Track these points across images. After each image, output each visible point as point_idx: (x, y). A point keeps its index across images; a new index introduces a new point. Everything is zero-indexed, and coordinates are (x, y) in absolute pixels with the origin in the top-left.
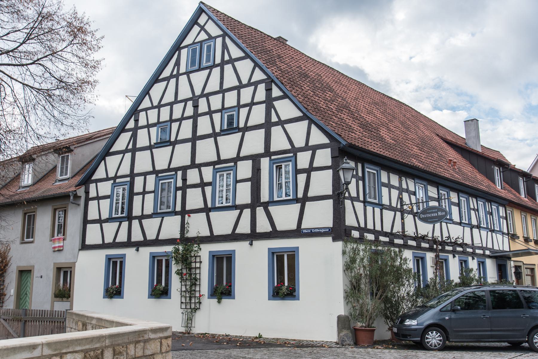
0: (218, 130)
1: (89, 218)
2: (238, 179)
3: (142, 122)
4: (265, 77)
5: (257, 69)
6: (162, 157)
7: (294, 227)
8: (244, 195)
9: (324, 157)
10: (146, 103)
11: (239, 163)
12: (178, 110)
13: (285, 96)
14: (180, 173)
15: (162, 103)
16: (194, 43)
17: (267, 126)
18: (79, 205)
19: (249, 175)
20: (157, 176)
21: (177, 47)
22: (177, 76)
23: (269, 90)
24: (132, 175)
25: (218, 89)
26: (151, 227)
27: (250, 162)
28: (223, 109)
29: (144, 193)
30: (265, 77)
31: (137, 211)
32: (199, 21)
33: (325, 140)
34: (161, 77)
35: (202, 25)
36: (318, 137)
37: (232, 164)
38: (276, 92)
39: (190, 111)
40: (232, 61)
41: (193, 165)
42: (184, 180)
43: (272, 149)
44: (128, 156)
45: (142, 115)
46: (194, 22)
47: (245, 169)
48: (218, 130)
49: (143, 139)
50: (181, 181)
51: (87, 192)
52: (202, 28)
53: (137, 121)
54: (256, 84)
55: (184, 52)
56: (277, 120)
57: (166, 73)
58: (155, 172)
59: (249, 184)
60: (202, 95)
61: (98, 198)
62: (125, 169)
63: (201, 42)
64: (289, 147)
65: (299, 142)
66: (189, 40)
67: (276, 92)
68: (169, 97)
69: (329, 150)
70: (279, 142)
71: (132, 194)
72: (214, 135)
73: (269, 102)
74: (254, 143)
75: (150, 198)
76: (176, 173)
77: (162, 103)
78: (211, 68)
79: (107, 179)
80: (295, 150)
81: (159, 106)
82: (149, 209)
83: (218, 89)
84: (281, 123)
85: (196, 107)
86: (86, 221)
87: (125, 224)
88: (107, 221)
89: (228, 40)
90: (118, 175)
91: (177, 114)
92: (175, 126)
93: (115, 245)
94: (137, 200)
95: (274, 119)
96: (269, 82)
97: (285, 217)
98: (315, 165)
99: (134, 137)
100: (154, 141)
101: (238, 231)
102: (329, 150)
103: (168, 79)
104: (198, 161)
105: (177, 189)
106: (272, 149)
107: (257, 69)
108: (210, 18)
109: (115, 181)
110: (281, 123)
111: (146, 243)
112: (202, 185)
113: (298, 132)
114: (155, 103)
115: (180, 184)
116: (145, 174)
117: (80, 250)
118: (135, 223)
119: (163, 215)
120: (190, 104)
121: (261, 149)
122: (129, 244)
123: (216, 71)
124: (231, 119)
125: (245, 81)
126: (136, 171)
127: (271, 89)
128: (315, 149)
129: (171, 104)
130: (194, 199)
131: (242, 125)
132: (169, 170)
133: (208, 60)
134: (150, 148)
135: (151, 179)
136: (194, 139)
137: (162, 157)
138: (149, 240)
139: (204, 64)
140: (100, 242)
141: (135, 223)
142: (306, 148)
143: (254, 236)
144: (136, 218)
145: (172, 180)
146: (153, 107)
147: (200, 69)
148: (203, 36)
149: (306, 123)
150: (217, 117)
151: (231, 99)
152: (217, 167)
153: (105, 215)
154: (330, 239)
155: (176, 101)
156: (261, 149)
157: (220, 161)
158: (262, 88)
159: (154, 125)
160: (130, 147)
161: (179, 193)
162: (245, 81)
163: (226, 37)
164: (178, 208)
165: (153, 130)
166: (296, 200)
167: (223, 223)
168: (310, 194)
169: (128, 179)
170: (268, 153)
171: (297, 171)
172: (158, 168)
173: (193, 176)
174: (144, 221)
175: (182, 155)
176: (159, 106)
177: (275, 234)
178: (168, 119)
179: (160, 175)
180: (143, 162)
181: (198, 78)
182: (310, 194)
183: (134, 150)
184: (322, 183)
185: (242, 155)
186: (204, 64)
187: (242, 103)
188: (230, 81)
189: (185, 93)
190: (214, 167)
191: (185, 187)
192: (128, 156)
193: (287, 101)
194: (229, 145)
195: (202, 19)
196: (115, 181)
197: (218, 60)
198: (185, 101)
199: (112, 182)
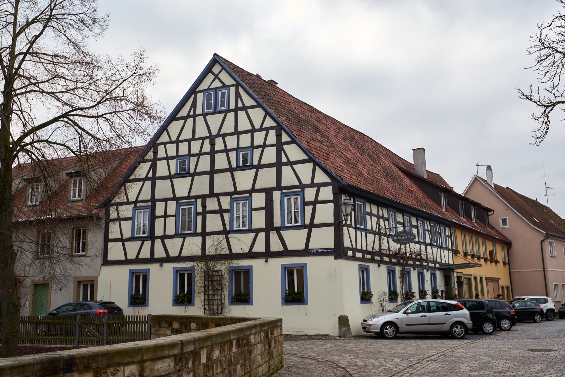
0: (234, 165)
1: (111, 236)
2: (253, 207)
3: (161, 153)
4: (276, 125)
5: (268, 117)
6: (182, 187)
7: (303, 247)
8: (259, 220)
9: (327, 193)
10: (164, 138)
11: (253, 194)
12: (196, 147)
13: (293, 142)
14: (199, 201)
15: (180, 139)
16: (209, 89)
17: (278, 165)
18: (100, 225)
19: (263, 205)
20: (177, 202)
21: (193, 91)
22: (194, 116)
23: (279, 136)
24: (153, 201)
25: (233, 130)
26: (174, 247)
27: (264, 194)
28: (238, 149)
29: (165, 216)
30: (276, 125)
31: (159, 232)
32: (213, 70)
33: (327, 180)
34: (178, 116)
35: (216, 73)
36: (321, 177)
37: (248, 195)
38: (285, 138)
39: (207, 147)
40: (245, 108)
41: (212, 194)
42: (204, 206)
43: (283, 184)
44: (148, 184)
45: (161, 149)
46: (208, 70)
47: (259, 200)
48: (234, 165)
49: (162, 169)
50: (201, 208)
51: (108, 214)
52: (216, 76)
53: (156, 153)
54: (268, 129)
55: (200, 96)
56: (286, 161)
57: (184, 112)
58: (175, 198)
59: (263, 212)
60: (219, 135)
61: (119, 220)
62: (146, 195)
63: (216, 89)
64: (298, 184)
65: (306, 180)
66: (204, 86)
67: (285, 138)
68: (187, 134)
69: (330, 188)
70: (288, 177)
71: (153, 217)
72: (231, 170)
73: (279, 146)
74: (267, 178)
75: (171, 222)
76: (196, 200)
77: (180, 139)
78: (226, 112)
79: (128, 203)
80: (302, 187)
81: (177, 142)
82: (171, 230)
83: (233, 130)
84: (290, 163)
85: (213, 144)
86: (107, 240)
87: (148, 244)
88: (129, 240)
89: (240, 90)
90: (139, 199)
91: (195, 149)
92: (193, 160)
93: (137, 261)
94: (159, 223)
95: (284, 160)
96: (279, 129)
97: (295, 239)
98: (320, 198)
99: (154, 167)
100: (173, 172)
101: (255, 250)
102: (330, 188)
103: (185, 118)
104: (216, 191)
105: (197, 214)
106: (283, 184)
107: (268, 117)
108: (223, 68)
109: (136, 205)
110: (290, 163)
111: (169, 259)
112: (221, 211)
113: (305, 171)
114: (174, 138)
115: (200, 209)
116: (166, 200)
117: (102, 265)
118: (158, 243)
119: (184, 236)
120: (207, 142)
121: (273, 184)
122: (152, 260)
123: (231, 115)
124: (245, 156)
125: (257, 126)
126: (157, 197)
127: (281, 135)
128: (319, 186)
129: (189, 141)
130: (214, 223)
131: (256, 163)
132: (189, 197)
133: (223, 105)
134: (170, 177)
135: (172, 205)
136: (212, 172)
137: (182, 187)
138: (172, 257)
139: (219, 108)
140: (123, 258)
141: (158, 243)
142: (312, 185)
143: (268, 254)
144: (158, 238)
145: (192, 206)
146: (171, 142)
147: (216, 112)
148: (217, 84)
149: (311, 165)
150: (233, 155)
151: (245, 141)
152: (233, 196)
153: (127, 234)
154: (332, 257)
155: (194, 138)
156: (273, 184)
157: (236, 192)
158: (272, 133)
159: (173, 158)
160: (150, 175)
161: (200, 218)
162: (257, 126)
163: (240, 87)
164: (199, 230)
165: (173, 163)
166: (304, 226)
167: (240, 243)
168: (316, 221)
169: (150, 204)
170: (279, 187)
171: (305, 204)
172: (178, 195)
173: (212, 204)
174: (166, 241)
175: (201, 186)
176: (177, 142)
177: (286, 253)
178: (187, 153)
179: (180, 201)
180: (163, 189)
181: (215, 121)
182: (316, 221)
183: (154, 179)
184: (325, 213)
185: (256, 187)
186: (219, 108)
187: (255, 144)
188: (244, 125)
189: (202, 131)
190: (231, 197)
191: (205, 213)
192: (148, 184)
193: (294, 146)
194: (244, 179)
195: (216, 69)
196: (136, 205)
197: (232, 106)
198: (203, 139)
199: (133, 205)
